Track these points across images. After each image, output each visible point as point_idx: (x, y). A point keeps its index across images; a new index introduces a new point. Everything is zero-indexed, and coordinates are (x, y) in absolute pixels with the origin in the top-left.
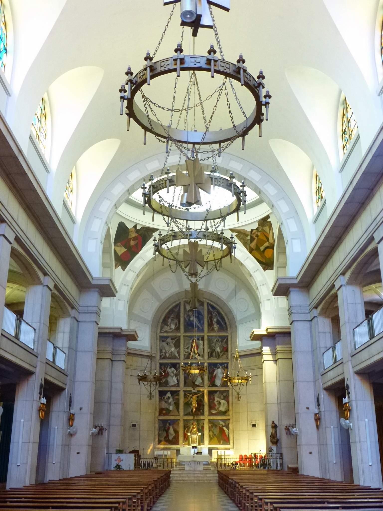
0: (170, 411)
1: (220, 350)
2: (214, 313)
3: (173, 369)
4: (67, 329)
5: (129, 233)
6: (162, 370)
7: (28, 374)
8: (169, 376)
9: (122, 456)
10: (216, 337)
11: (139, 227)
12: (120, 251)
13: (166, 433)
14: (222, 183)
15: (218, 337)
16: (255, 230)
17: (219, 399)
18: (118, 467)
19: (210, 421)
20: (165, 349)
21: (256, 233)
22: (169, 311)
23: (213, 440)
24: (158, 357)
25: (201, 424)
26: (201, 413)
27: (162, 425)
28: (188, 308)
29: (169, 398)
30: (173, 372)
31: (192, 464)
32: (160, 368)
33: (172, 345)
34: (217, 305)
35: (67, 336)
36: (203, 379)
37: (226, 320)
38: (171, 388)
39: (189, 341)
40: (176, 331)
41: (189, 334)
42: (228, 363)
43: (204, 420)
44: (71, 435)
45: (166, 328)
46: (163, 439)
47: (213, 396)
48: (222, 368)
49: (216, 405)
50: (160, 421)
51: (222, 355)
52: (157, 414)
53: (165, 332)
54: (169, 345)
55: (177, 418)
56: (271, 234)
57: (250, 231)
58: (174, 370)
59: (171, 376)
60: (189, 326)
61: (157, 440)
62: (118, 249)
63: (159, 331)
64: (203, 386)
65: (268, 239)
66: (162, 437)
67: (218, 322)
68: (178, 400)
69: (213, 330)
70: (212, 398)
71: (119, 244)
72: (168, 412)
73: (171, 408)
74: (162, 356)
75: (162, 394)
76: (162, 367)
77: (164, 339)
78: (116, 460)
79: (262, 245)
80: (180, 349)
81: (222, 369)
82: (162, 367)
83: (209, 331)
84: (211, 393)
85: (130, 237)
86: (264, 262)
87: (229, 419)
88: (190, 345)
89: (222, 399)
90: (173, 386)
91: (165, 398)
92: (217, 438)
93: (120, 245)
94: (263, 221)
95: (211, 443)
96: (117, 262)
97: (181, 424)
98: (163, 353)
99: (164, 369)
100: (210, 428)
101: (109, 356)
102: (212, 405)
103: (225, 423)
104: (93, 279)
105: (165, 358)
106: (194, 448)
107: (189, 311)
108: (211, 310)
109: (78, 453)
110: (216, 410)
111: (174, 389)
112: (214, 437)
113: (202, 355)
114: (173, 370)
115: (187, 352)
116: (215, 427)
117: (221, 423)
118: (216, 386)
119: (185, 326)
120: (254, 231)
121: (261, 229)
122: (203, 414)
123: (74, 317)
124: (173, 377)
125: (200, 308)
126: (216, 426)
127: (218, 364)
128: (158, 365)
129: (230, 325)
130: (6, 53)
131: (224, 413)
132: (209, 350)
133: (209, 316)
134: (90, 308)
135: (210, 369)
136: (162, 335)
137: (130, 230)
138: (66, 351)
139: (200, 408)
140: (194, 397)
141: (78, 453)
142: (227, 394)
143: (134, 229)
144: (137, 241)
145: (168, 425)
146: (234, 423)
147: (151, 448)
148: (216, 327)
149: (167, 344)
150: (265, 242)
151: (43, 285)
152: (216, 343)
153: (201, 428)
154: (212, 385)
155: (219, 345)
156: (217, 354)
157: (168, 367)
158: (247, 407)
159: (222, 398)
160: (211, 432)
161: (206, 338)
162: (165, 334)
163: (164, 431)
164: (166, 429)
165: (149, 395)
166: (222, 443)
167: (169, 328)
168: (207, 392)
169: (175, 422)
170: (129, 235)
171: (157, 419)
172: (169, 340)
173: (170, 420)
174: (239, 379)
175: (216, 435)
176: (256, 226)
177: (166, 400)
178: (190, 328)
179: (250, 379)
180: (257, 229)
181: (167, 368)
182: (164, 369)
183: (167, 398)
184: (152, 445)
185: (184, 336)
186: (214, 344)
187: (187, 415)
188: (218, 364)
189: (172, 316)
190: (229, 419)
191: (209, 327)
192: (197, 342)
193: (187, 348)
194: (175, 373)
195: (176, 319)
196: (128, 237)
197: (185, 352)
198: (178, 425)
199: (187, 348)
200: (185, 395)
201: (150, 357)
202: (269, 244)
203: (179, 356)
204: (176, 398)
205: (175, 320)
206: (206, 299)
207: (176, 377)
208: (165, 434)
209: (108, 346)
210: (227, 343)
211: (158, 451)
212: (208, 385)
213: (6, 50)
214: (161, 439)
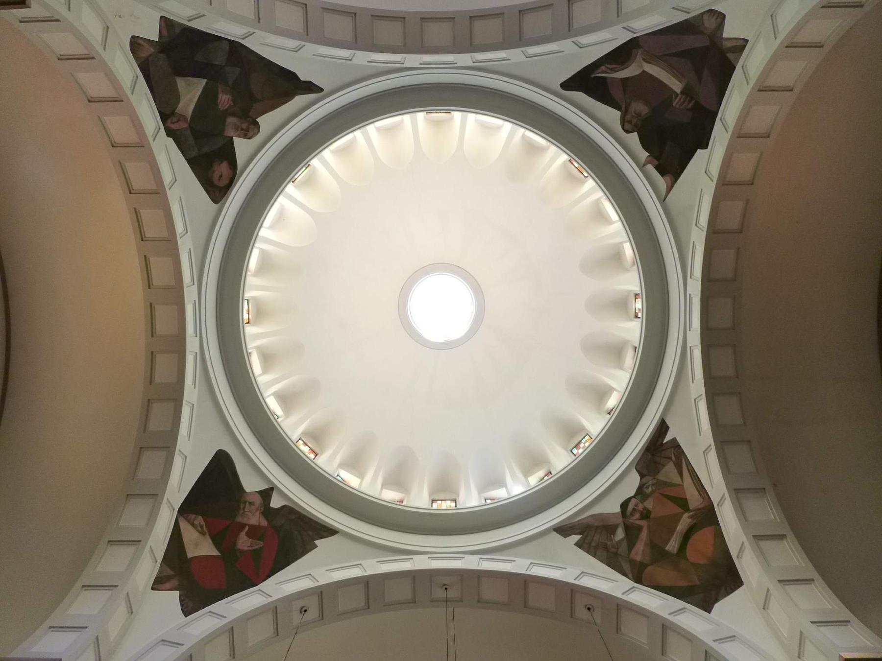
5: (242, 506)
11: (276, 502)
12: (197, 545)
16: (633, 501)
21: (640, 507)
56: (688, 481)
62: (189, 534)
65: (683, 503)
71: (200, 520)
79: (672, 531)
86: (696, 586)
93: (201, 527)
94: (650, 456)
96: (170, 572)
120: (631, 507)
121: (653, 485)
137: (250, 499)
143: (258, 500)
144: (261, 542)
150: (680, 516)
170: (241, 512)
176: (634, 481)
180: (640, 490)
202: (690, 517)
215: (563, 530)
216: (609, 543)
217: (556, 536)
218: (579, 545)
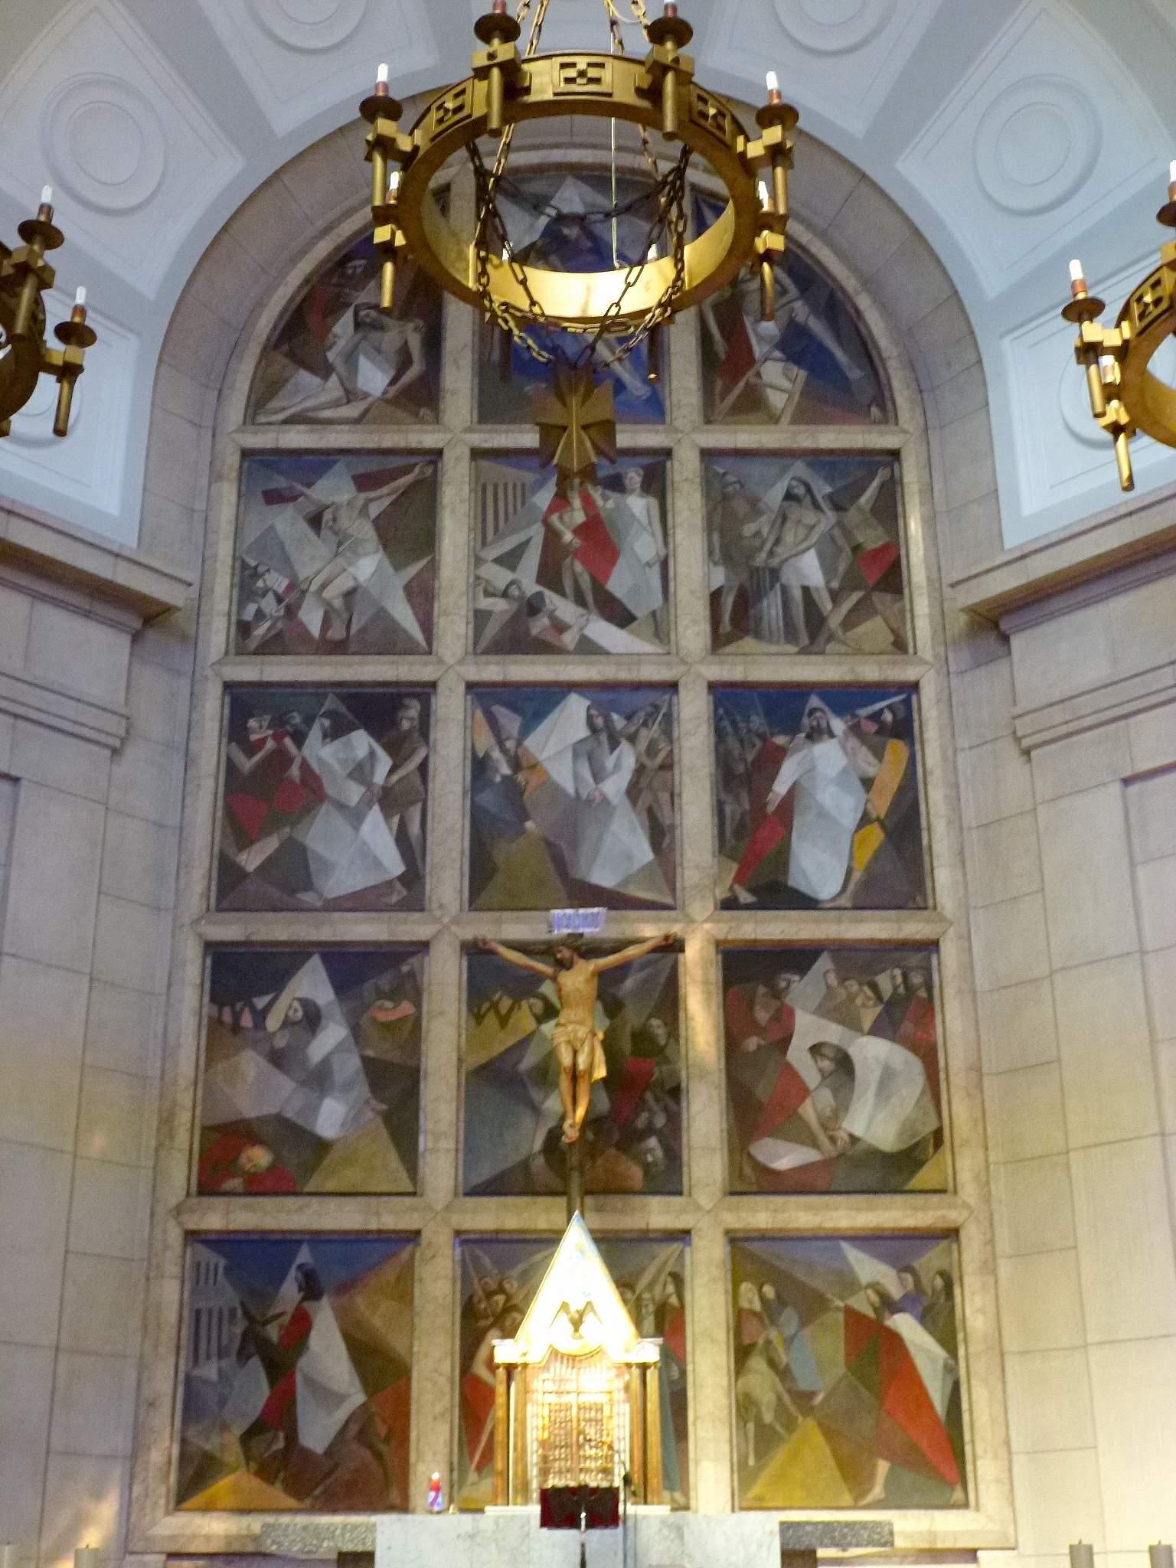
0: (322, 1147)
1: (828, 569)
3: (361, 742)
6: (250, 749)
8: (325, 807)
10: (784, 470)
13: (272, 1383)
15: (800, 469)
17: (832, 1033)
20: (286, 563)
23: (779, 1457)
24: (217, 635)
25: (650, 1286)
26: (647, 1167)
27: (226, 1296)
29: (312, 1019)
30: (360, 772)
32: (236, 731)
33: (368, 532)
36: (660, 835)
38: (337, 915)
39: (525, 493)
40: (400, 414)
42: (914, 687)
43: (683, 1236)
46: (227, 1445)
47: (777, 994)
48: (855, 729)
49: (804, 1092)
51: (848, 624)
52: (179, 1174)
54: (325, 532)
55: (391, 1217)
58: (372, 754)
59: (341, 806)
61: (163, 1451)
64: (669, 900)
66: (225, 1428)
68: (412, 1034)
69: (752, 404)
70: (762, 1016)
74: (260, 631)
76: (252, 723)
77: (280, 482)
80: (433, 568)
81: (853, 742)
82: (258, 727)
87: (952, 1234)
88: (536, 533)
89: (867, 1024)
91: (273, 1023)
92: (830, 1434)
95: (755, 1490)
98: (269, 604)
99: (270, 744)
100: (751, 1327)
102: (763, 1091)
106: (572, 1522)
110: (815, 1144)
112: (790, 1425)
113: (654, 614)
114: (361, 752)
115: (505, 594)
116: (805, 1321)
117: (868, 1268)
118: (805, 902)
119: (482, 368)
124: (356, 817)
126: (812, 1306)
127: (815, 701)
128: (213, 708)
129: (911, 366)
132: (719, 577)
135: (733, 743)
139: (641, 1121)
142: (917, 979)
145: (290, 1291)
146: (1004, 1269)
149: (315, 521)
154: (752, 891)
155: (812, 528)
157: (309, 720)
158: (1158, 1090)
159: (869, 1017)
160: (757, 1363)
161: (685, 469)
162: (297, 438)
163: (243, 1356)
164: (273, 1332)
168: (712, 950)
171: (175, 1235)
173: (317, 1238)
177: (280, 1042)
181: (299, 738)
183: (287, 1023)
184: (107, 1511)
185: (477, 454)
186: (763, 524)
188: (815, 701)
190: (952, 1234)
191: (719, 385)
192: (605, 502)
193: (510, 560)
194: (380, 776)
197: (488, 594)
198: (404, 1291)
199: (510, 560)
203: (429, 640)
204: (382, 1017)
207: (387, 816)
210: (888, 510)
212: (721, 893)
214: (211, 1445)
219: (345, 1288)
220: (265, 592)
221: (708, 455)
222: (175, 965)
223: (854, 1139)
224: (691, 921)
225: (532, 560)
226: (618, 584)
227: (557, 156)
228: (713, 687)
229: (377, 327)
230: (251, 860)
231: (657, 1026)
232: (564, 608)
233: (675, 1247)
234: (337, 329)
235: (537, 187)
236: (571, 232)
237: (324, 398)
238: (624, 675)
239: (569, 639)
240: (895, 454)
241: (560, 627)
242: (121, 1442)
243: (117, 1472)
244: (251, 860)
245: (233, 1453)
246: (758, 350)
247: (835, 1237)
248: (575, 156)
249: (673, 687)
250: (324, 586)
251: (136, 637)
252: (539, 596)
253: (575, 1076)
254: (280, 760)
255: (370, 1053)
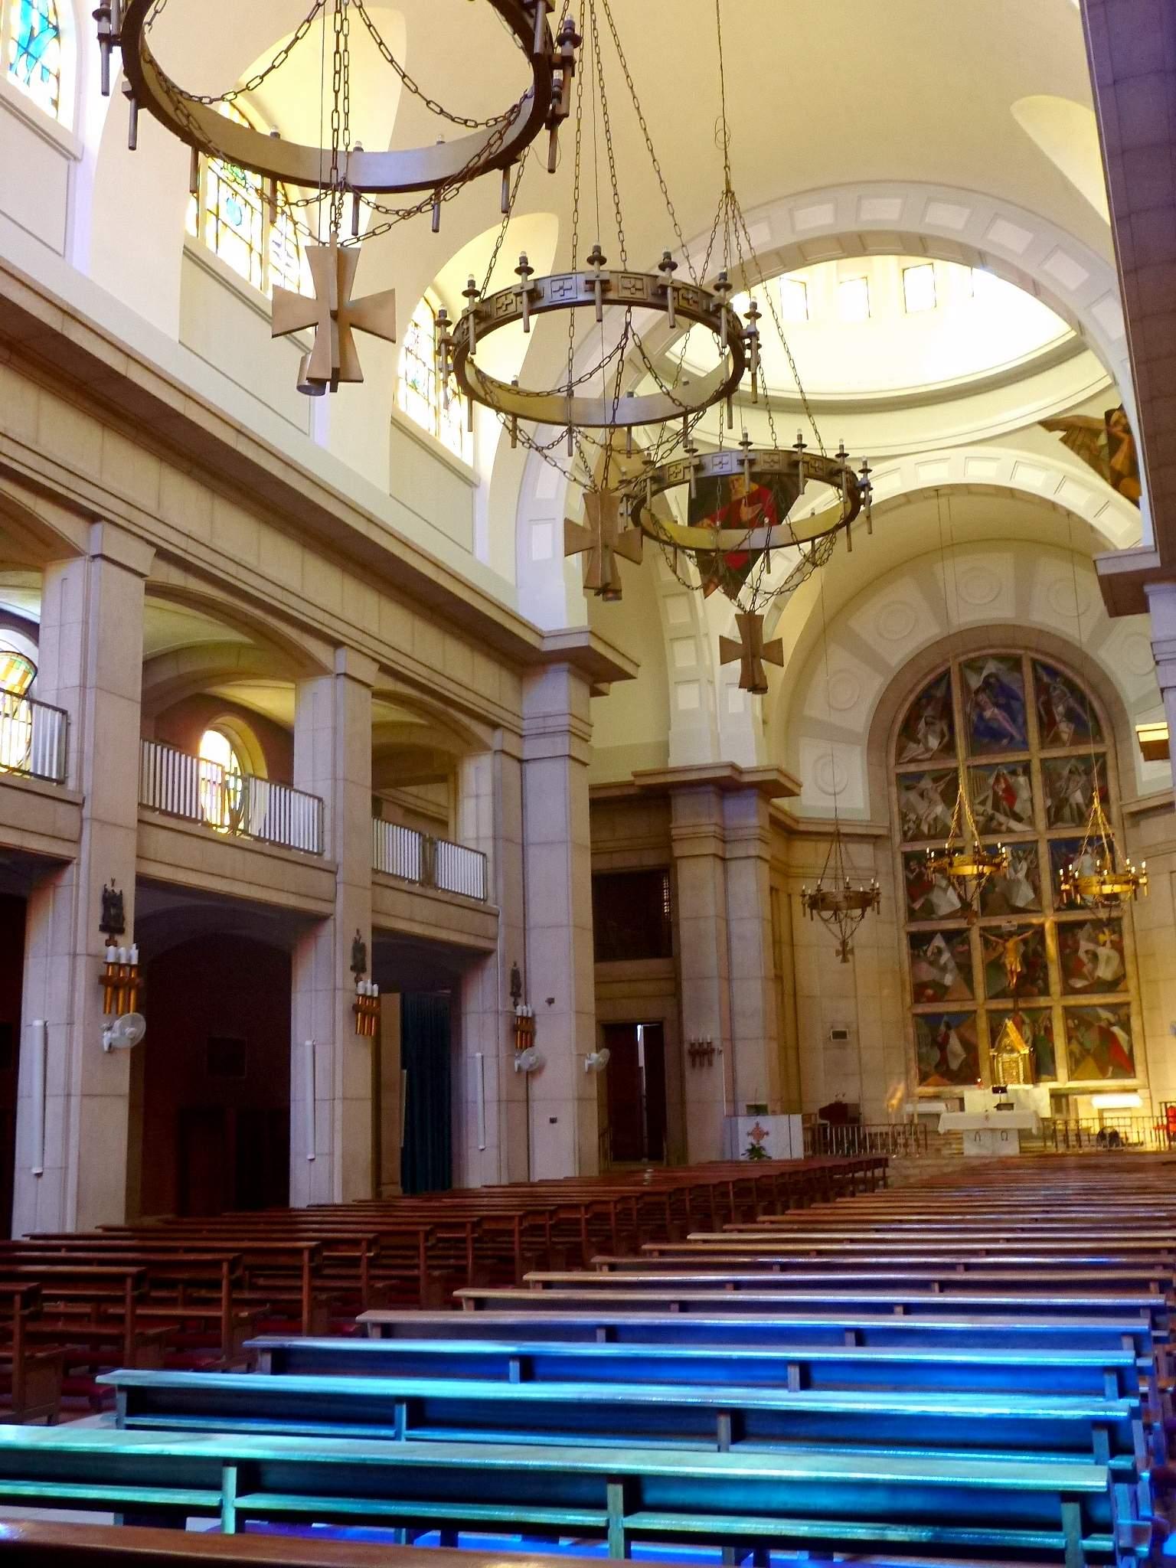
0: (946, 988)
2: (1055, 688)
4: (486, 787)
5: (731, 487)
6: (912, 871)
7: (311, 922)
9: (767, 1122)
10: (1068, 762)
14: (633, 290)
15: (1073, 761)
17: (1091, 946)
18: (756, 1151)
19: (1069, 1012)
20: (914, 810)
22: (919, 699)
24: (897, 838)
25: (1043, 1022)
27: (925, 1030)
28: (975, 682)
29: (940, 951)
31: (986, 1139)
33: (937, 797)
34: (1065, 663)
35: (486, 804)
36: (1036, 889)
37: (1096, 705)
38: (943, 922)
41: (983, 760)
43: (1050, 1008)
44: (530, 1074)
45: (914, 749)
47: (1074, 936)
50: (920, 1020)
52: (908, 999)
53: (912, 761)
55: (968, 1006)
57: (1103, 417)
59: (940, 887)
60: (985, 736)
61: (914, 1072)
63: (892, 760)
67: (1071, 716)
68: (968, 954)
69: (1056, 740)
70: (1070, 942)
72: (941, 992)
73: (948, 979)
74: (910, 833)
75: (917, 941)
77: (908, 783)
78: (749, 1134)
82: (913, 864)
83: (1043, 746)
84: (1063, 929)
85: (734, 498)
87: (1128, 1004)
88: (990, 793)
90: (951, 916)
91: (929, 953)
95: (1076, 1075)
97: (983, 1024)
98: (911, 824)
101: (711, 847)
103: (1114, 1013)
104: (543, 637)
105: (918, 837)
106: (997, 1092)
107: (977, 692)
108: (1046, 679)
109: (553, 1121)
110: (1086, 979)
111: (951, 925)
115: (982, 815)
116: (1087, 1030)
117: (1105, 1015)
120: (1114, 417)
122: (1045, 991)
123: (503, 752)
124: (945, 890)
125: (1008, 679)
126: (1089, 1025)
128: (899, 860)
129: (1110, 720)
130: (57, 36)
131: (1114, 985)
133: (1042, 698)
134: (550, 722)
136: (901, 770)
138: (487, 847)
140: (1010, 944)
141: (553, 1121)
145: (943, 1028)
146: (1145, 1013)
147: (899, 1095)
148: (1065, 729)
149: (922, 795)
151: (333, 675)
152: (1069, 779)
153: (1042, 1033)
155: (1078, 782)
156: (1076, 813)
160: (1074, 1041)
161: (1036, 766)
162: (912, 768)
163: (932, 1046)
164: (940, 1039)
165: (841, 949)
166: (1112, 1072)
167: (923, 750)
168: (1053, 925)
169: (965, 1018)
171: (910, 1015)
172: (926, 784)
173: (948, 1013)
174: (1103, 883)
175: (1092, 1051)
177: (932, 959)
178: (986, 740)
179: (1142, 881)
182: (917, 870)
183: (933, 953)
184: (901, 1087)
186: (1062, 783)
187: (996, 996)
189: (929, 712)
190: (1128, 1004)
192: (1011, 780)
193: (983, 803)
195: (941, 719)
196: (730, 497)
197: (977, 815)
198: (973, 1026)
199: (983, 803)
200: (986, 943)
201: (874, 839)
205: (937, 722)
206: (1026, 648)
208: (936, 1055)
209: (704, 820)
210: (1103, 773)
211: (919, 1102)
212: (1056, 906)
213: (56, 28)
215: (1049, 424)
216: (1092, 445)
217: (1041, 429)
218: (1064, 440)
219: (957, 1027)
220: (909, 821)
221: (1043, 761)
222: (899, 939)
223: (1099, 978)
224: (1046, 917)
225: (990, 803)
226: (1017, 808)
227: (985, 652)
228: (1049, 841)
229: (933, 724)
230: (917, 906)
231: (1039, 948)
232: (1001, 818)
233: (1048, 1011)
234: (920, 726)
235: (980, 664)
236: (992, 680)
237: (919, 752)
238: (1021, 840)
239: (1004, 828)
240: (1104, 755)
241: (1000, 824)
242: (903, 1069)
243: (903, 1077)
244: (917, 906)
245: (933, 1070)
246: (1058, 718)
247: (1095, 1006)
248: (991, 651)
249: (1036, 842)
250: (927, 817)
251: (874, 844)
252: (993, 814)
253: (1012, 972)
254: (920, 875)
255: (958, 961)
